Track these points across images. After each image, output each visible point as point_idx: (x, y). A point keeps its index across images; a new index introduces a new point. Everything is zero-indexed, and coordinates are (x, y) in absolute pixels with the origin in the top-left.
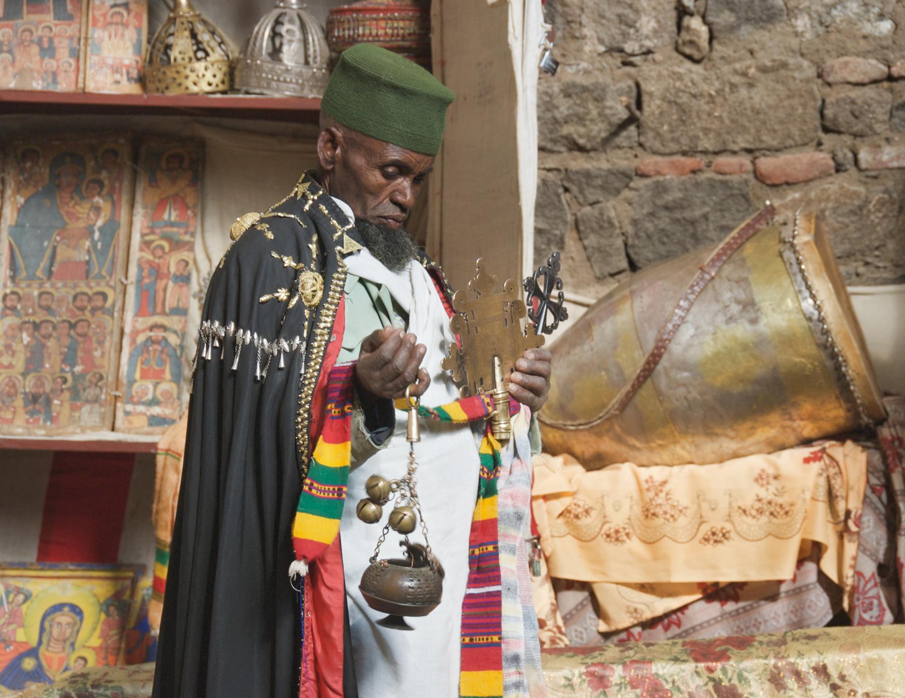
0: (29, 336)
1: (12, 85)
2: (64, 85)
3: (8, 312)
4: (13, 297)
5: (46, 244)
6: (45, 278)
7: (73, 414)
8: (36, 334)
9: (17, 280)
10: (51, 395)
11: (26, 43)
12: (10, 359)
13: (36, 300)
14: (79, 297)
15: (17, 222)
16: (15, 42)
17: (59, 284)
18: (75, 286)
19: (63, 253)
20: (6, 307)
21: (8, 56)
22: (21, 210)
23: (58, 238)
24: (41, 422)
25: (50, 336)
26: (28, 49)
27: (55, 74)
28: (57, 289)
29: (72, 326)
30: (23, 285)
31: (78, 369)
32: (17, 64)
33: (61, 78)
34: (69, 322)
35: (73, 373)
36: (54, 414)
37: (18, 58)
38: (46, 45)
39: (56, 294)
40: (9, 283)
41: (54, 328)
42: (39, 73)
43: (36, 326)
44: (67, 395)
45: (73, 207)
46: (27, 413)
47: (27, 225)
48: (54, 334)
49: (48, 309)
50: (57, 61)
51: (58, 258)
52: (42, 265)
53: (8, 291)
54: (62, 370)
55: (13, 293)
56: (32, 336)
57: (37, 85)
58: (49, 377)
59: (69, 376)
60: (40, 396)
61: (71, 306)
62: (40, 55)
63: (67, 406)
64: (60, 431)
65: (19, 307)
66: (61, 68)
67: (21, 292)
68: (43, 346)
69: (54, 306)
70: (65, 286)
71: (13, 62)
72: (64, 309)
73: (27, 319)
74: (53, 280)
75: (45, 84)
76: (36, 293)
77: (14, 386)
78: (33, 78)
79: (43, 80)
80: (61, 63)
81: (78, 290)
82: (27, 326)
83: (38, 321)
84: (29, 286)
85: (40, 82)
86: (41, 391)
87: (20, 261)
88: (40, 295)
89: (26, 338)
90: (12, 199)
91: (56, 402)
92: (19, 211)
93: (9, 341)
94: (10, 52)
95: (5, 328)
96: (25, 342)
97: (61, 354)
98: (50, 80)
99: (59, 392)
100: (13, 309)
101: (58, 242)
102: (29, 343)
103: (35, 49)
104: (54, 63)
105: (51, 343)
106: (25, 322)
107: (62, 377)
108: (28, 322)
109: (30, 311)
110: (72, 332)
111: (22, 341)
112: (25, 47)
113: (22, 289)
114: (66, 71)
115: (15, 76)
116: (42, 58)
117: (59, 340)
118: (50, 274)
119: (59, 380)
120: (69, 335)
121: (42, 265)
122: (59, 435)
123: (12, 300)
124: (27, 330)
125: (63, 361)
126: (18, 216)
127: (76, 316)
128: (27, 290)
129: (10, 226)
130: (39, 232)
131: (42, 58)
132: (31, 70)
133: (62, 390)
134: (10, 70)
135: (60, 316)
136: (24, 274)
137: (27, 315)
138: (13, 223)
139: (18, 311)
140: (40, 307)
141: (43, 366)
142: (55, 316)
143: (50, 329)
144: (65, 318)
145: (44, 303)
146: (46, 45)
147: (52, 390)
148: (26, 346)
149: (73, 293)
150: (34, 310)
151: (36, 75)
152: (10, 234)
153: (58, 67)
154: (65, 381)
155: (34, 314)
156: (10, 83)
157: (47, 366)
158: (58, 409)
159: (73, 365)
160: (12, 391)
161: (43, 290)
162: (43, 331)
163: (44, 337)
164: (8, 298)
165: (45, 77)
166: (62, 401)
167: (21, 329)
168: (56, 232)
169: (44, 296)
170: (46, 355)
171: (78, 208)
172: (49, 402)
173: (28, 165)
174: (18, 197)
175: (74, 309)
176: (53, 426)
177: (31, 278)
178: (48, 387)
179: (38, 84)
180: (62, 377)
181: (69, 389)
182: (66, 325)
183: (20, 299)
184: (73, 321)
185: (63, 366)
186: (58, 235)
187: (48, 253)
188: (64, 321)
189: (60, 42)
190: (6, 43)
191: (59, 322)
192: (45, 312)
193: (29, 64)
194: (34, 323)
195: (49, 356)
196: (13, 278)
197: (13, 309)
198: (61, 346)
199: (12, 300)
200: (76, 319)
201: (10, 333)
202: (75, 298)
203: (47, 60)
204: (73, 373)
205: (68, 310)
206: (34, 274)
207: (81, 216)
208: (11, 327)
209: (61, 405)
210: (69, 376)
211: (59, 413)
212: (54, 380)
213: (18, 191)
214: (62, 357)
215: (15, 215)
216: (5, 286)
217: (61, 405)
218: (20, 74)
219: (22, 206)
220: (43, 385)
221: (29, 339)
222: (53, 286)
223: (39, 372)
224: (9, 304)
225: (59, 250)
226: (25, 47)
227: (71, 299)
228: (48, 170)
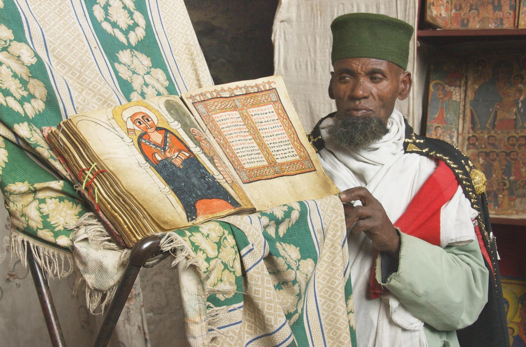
0: (483, 159)
1: (478, 27)
2: (507, 25)
3: (471, 146)
4: (474, 138)
5: (491, 110)
6: (491, 128)
7: (510, 203)
8: (487, 158)
9: (475, 129)
10: (497, 192)
11: (485, 4)
13: (487, 140)
14: (511, 139)
15: (474, 98)
16: (479, 4)
17: (499, 132)
18: (509, 133)
19: (501, 115)
20: (469, 144)
21: (476, 12)
22: (476, 92)
23: (498, 107)
24: (492, 206)
25: (495, 159)
26: (486, 7)
27: (501, 20)
28: (498, 134)
29: (508, 154)
30: (479, 132)
31: (512, 178)
32: (481, 16)
33: (504, 22)
34: (506, 153)
35: (509, 180)
36: (500, 203)
37: (481, 12)
38: (496, 4)
39: (498, 137)
40: (471, 131)
41: (497, 155)
42: (493, 19)
43: (487, 154)
44: (506, 192)
45: (506, 90)
47: (480, 100)
48: (498, 159)
49: (493, 145)
50: (503, 12)
51: (498, 118)
52: (489, 121)
53: (471, 135)
54: (503, 179)
55: (473, 136)
56: (484, 159)
57: (492, 26)
58: (495, 182)
59: (507, 182)
60: (491, 192)
61: (506, 143)
62: (493, 10)
63: (507, 198)
64: (504, 212)
65: (477, 144)
66: (505, 16)
67: (477, 136)
68: (492, 165)
69: (496, 144)
70: (502, 132)
71: (478, 15)
72: (502, 145)
73: (481, 150)
74: (496, 129)
75: (496, 25)
76: (486, 136)
78: (489, 23)
79: (495, 23)
80: (505, 13)
81: (510, 135)
82: (482, 154)
83: (488, 151)
84: (482, 133)
85: (493, 24)
86: (491, 189)
87: (477, 119)
88: (489, 137)
89: (481, 161)
90: (472, 87)
91: (500, 196)
92: (476, 93)
94: (477, 9)
96: (481, 163)
97: (502, 169)
98: (499, 23)
99: (502, 191)
100: (474, 145)
101: (498, 109)
102: (483, 163)
103: (490, 7)
104: (501, 14)
105: (496, 164)
106: (481, 152)
107: (503, 182)
108: (482, 152)
109: (483, 146)
110: (508, 158)
111: (479, 162)
112: (484, 6)
113: (478, 134)
114: (508, 18)
115: (479, 22)
116: (494, 11)
117: (500, 162)
118: (494, 126)
119: (501, 184)
120: (506, 160)
121: (489, 121)
122: (503, 214)
123: (473, 140)
124: (482, 156)
125: (503, 173)
126: (475, 95)
128: (481, 135)
129: (471, 101)
130: (487, 103)
131: (494, 11)
132: (488, 18)
133: (503, 190)
134: (477, 18)
135: (500, 149)
136: (479, 126)
137: (482, 148)
138: (473, 99)
139: (477, 146)
140: (489, 144)
141: (492, 176)
142: (497, 149)
143: (495, 156)
144: (503, 150)
145: (491, 142)
146: (496, 4)
147: (497, 189)
148: (482, 165)
149: (508, 136)
150: (485, 145)
151: (491, 21)
152: (471, 105)
153: (503, 15)
154: (505, 185)
155: (485, 148)
156: (477, 26)
157: (494, 176)
158: (501, 200)
159: (509, 176)
161: (490, 135)
162: (491, 157)
163: (492, 160)
164: (471, 139)
165: (496, 21)
166: (504, 196)
167: (478, 155)
168: (497, 104)
169: (491, 138)
170: (493, 170)
171: (508, 90)
172: (496, 196)
173: (480, 68)
174: (475, 85)
175: (508, 145)
176: (499, 209)
177: (483, 128)
178: (495, 189)
179: (492, 25)
180: (503, 182)
181: (507, 189)
182: (504, 154)
183: (477, 140)
184: (508, 152)
185: (503, 176)
186: (498, 105)
187: (492, 115)
188: (503, 152)
189: (505, 2)
190: (474, 4)
191: (499, 152)
192: (492, 147)
193: (487, 15)
194: (486, 152)
195: (495, 171)
196: (473, 128)
197: (474, 145)
199: (473, 140)
200: (510, 151)
202: (509, 139)
203: (497, 12)
204: (509, 180)
205: (505, 145)
206: (485, 126)
207: (511, 94)
209: (503, 198)
210: (507, 182)
211: (502, 202)
212: (499, 184)
213: (475, 82)
214: (502, 171)
215: (474, 95)
216: (469, 133)
217: (503, 198)
218: (482, 21)
219: (477, 90)
220: (492, 186)
221: (483, 161)
222: (496, 132)
223: (490, 179)
224: (471, 142)
225: (498, 113)
226: (484, 6)
227: (506, 140)
228: (491, 71)
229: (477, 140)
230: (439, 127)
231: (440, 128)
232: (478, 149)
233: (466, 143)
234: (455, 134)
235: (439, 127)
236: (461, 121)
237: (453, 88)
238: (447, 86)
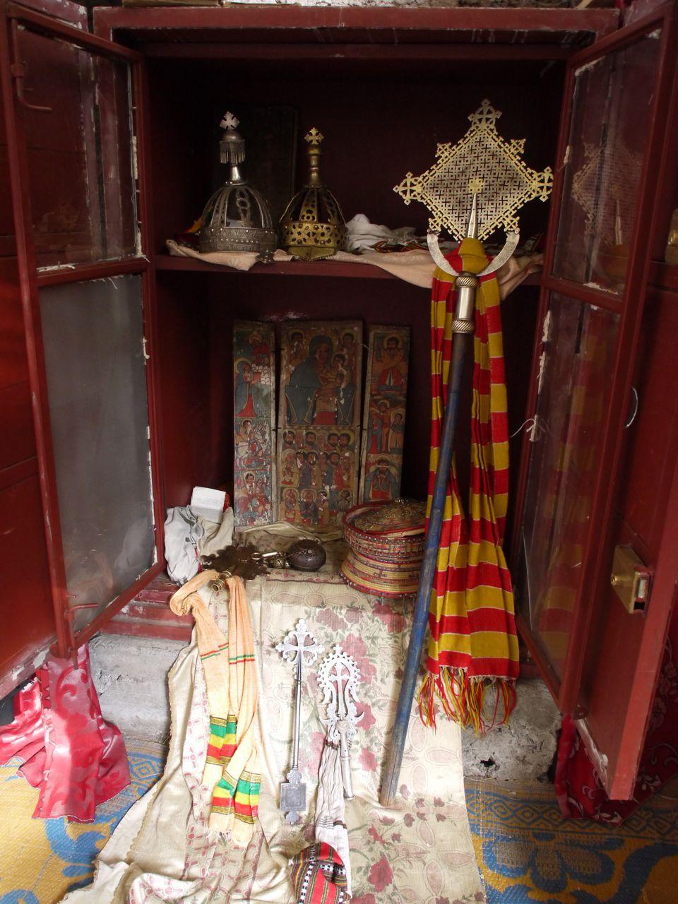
12: (290, 478)
13: (305, 438)
29: (328, 457)
46: (302, 515)
49: (311, 444)
58: (315, 491)
67: (294, 432)
68: (311, 470)
77: (293, 496)
81: (331, 432)
84: (300, 428)
86: (311, 501)
88: (307, 434)
92: (291, 376)
93: (289, 466)
95: (286, 456)
101: (317, 398)
106: (298, 453)
113: (296, 429)
117: (320, 467)
124: (300, 458)
127: (331, 450)
140: (307, 442)
145: (309, 440)
148: (300, 469)
160: (292, 499)
174: (290, 366)
183: (294, 437)
187: (311, 405)
194: (304, 454)
196: (289, 422)
198: (321, 471)
201: (289, 460)
205: (325, 444)
208: (289, 455)
216: (285, 428)
219: (293, 372)
220: (311, 497)
222: (315, 428)
225: (318, 403)
227: (326, 439)
229: (294, 437)
230: (248, 421)
231: (249, 423)
232: (294, 449)
233: (281, 442)
234: (267, 430)
235: (248, 421)
236: (273, 412)
237: (261, 367)
238: (254, 365)
